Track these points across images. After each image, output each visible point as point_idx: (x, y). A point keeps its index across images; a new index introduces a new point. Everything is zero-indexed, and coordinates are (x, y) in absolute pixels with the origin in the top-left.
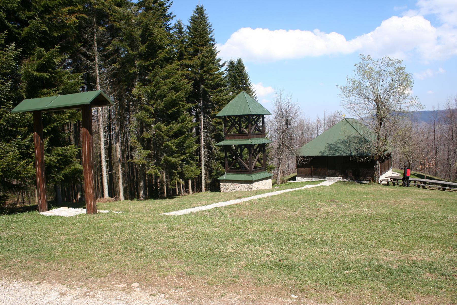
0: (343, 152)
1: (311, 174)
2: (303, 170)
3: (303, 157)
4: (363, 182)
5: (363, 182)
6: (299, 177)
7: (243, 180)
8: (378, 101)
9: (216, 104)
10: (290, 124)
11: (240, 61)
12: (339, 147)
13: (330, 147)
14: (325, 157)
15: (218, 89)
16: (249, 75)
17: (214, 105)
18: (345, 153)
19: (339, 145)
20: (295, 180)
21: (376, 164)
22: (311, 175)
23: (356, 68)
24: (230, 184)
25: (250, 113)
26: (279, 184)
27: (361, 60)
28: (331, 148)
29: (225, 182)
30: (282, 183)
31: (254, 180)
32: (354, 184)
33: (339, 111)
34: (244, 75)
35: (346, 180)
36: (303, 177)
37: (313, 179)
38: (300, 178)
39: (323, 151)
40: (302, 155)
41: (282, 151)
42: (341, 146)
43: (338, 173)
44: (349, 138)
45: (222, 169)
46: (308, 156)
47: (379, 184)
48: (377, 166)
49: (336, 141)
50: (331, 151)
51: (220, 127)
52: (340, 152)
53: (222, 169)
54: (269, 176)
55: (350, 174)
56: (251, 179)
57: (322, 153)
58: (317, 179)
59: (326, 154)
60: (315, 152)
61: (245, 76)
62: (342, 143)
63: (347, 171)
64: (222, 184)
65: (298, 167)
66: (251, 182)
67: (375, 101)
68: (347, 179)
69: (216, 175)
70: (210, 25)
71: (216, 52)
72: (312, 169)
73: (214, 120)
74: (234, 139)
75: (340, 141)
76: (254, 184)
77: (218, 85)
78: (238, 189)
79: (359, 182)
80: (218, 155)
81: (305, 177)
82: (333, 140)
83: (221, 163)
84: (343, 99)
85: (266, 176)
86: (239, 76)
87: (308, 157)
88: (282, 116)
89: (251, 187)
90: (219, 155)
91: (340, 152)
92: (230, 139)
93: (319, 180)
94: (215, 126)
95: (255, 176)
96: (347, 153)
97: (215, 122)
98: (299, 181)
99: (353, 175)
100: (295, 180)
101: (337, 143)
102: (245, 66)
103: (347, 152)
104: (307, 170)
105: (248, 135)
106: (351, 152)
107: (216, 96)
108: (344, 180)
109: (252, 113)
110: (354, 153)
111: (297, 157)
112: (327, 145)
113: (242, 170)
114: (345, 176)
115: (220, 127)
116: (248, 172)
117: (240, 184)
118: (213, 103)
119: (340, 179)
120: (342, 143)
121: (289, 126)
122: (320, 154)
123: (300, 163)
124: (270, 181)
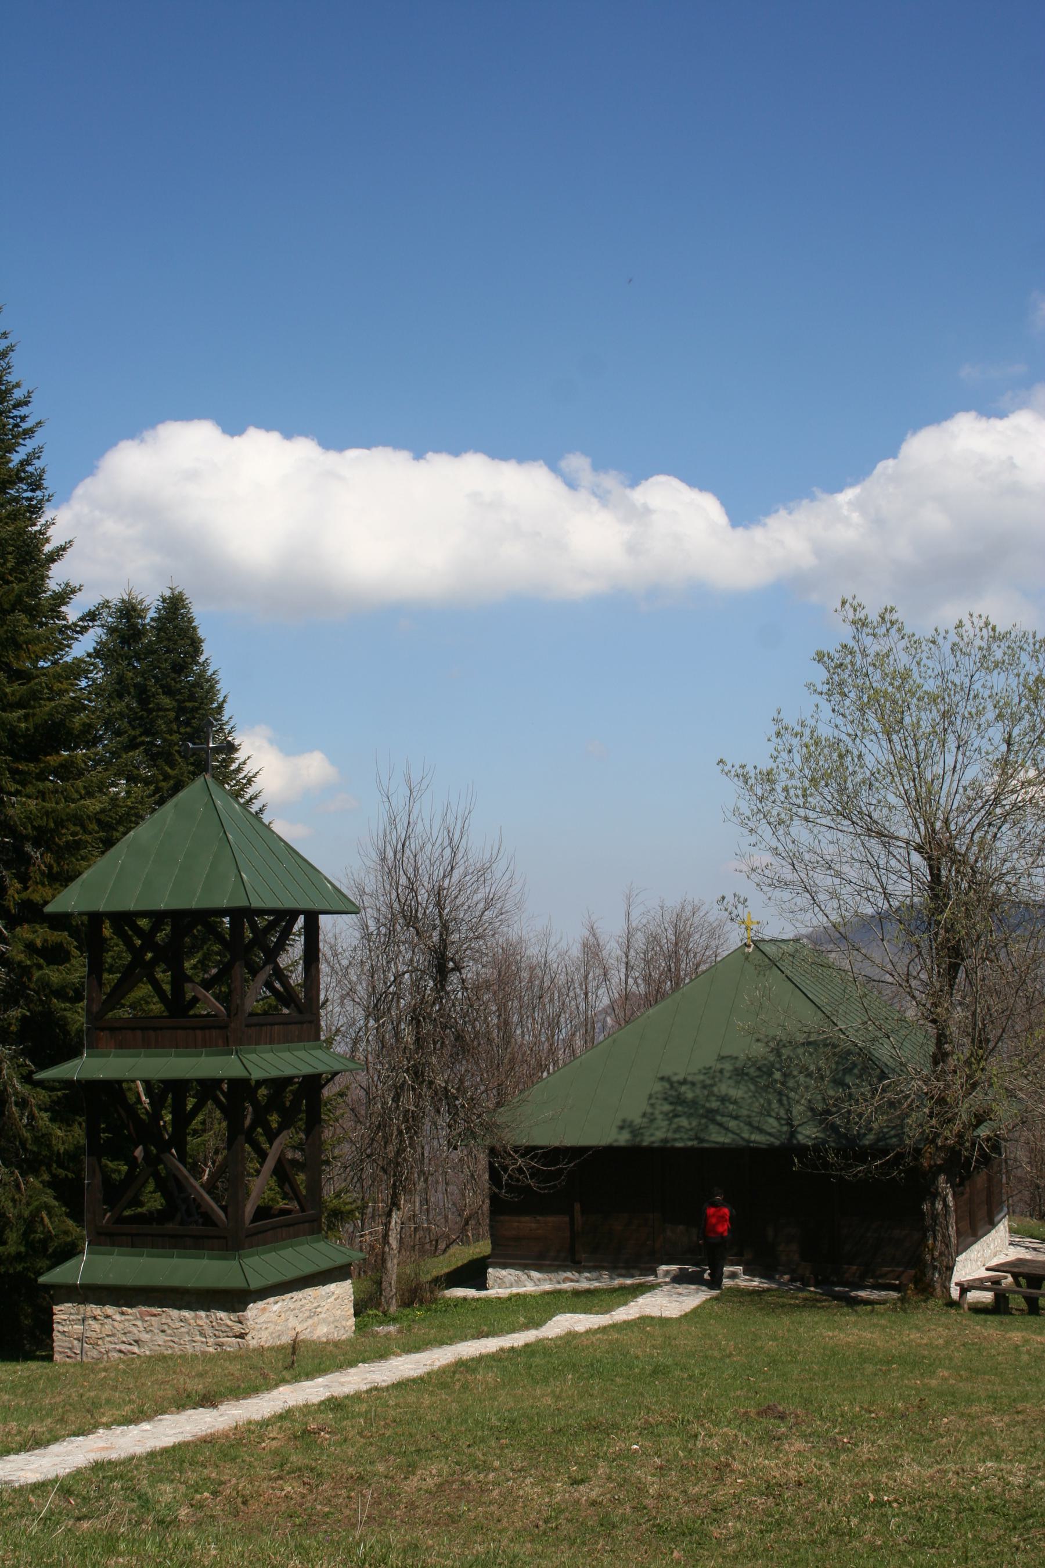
0: (750, 1123)
2: (527, 1224)
3: (529, 1151)
4: (863, 1294)
5: (863, 1294)
6: (504, 1266)
7: (191, 1284)
8: (936, 849)
9: (37, 845)
10: (458, 968)
11: (175, 606)
12: (724, 1099)
13: (675, 1096)
14: (650, 1150)
15: (53, 760)
16: (224, 688)
17: (28, 848)
18: (761, 1131)
19: (724, 1088)
20: (482, 1286)
21: (935, 1195)
22: (569, 1258)
23: (820, 674)
24: (110, 1310)
25: (242, 903)
26: (393, 1309)
27: (849, 630)
28: (679, 1100)
29: (84, 1301)
30: (407, 1303)
31: (255, 1284)
32: (810, 1304)
33: (730, 898)
34: (197, 684)
36: (524, 1267)
37: (585, 1282)
39: (638, 1121)
40: (524, 1141)
41: (413, 1120)
42: (736, 1093)
45: (56, 1223)
46: (557, 1150)
47: (952, 1304)
48: (939, 1206)
50: (684, 1122)
51: (54, 975)
52: (732, 1124)
53: (56, 1223)
54: (341, 1260)
56: (238, 1283)
57: (635, 1132)
58: (603, 1281)
59: (656, 1135)
60: (596, 1128)
61: (199, 693)
62: (740, 1074)
64: (64, 1313)
65: (498, 1207)
66: (236, 1300)
67: (919, 849)
68: (769, 1277)
69: (19, 1257)
70: (18, 394)
71: (47, 548)
73: (24, 932)
74: (147, 1045)
75: (728, 1066)
76: (253, 1310)
77: (55, 735)
78: (161, 1339)
79: (837, 1297)
80: (36, 1140)
81: (539, 1269)
83: (55, 1184)
84: (753, 839)
85: (325, 1265)
86: (168, 692)
87: (554, 1154)
88: (411, 920)
89: (237, 1328)
90: (43, 1139)
91: (732, 1124)
92: (120, 1045)
93: (617, 1282)
94: (26, 971)
95: (261, 1265)
96: (768, 1132)
97: (30, 947)
98: (504, 1292)
100: (482, 1286)
101: (714, 1075)
102: (201, 633)
105: (224, 1027)
107: (42, 795)
108: (756, 1283)
109: (256, 903)
110: (808, 1133)
111: (493, 1151)
112: (658, 1087)
113: (183, 1224)
115: (54, 975)
116: (227, 1241)
117: (175, 1313)
118: (20, 838)
120: (740, 1074)
122: (623, 1139)
123: (510, 1188)
124: (343, 1291)
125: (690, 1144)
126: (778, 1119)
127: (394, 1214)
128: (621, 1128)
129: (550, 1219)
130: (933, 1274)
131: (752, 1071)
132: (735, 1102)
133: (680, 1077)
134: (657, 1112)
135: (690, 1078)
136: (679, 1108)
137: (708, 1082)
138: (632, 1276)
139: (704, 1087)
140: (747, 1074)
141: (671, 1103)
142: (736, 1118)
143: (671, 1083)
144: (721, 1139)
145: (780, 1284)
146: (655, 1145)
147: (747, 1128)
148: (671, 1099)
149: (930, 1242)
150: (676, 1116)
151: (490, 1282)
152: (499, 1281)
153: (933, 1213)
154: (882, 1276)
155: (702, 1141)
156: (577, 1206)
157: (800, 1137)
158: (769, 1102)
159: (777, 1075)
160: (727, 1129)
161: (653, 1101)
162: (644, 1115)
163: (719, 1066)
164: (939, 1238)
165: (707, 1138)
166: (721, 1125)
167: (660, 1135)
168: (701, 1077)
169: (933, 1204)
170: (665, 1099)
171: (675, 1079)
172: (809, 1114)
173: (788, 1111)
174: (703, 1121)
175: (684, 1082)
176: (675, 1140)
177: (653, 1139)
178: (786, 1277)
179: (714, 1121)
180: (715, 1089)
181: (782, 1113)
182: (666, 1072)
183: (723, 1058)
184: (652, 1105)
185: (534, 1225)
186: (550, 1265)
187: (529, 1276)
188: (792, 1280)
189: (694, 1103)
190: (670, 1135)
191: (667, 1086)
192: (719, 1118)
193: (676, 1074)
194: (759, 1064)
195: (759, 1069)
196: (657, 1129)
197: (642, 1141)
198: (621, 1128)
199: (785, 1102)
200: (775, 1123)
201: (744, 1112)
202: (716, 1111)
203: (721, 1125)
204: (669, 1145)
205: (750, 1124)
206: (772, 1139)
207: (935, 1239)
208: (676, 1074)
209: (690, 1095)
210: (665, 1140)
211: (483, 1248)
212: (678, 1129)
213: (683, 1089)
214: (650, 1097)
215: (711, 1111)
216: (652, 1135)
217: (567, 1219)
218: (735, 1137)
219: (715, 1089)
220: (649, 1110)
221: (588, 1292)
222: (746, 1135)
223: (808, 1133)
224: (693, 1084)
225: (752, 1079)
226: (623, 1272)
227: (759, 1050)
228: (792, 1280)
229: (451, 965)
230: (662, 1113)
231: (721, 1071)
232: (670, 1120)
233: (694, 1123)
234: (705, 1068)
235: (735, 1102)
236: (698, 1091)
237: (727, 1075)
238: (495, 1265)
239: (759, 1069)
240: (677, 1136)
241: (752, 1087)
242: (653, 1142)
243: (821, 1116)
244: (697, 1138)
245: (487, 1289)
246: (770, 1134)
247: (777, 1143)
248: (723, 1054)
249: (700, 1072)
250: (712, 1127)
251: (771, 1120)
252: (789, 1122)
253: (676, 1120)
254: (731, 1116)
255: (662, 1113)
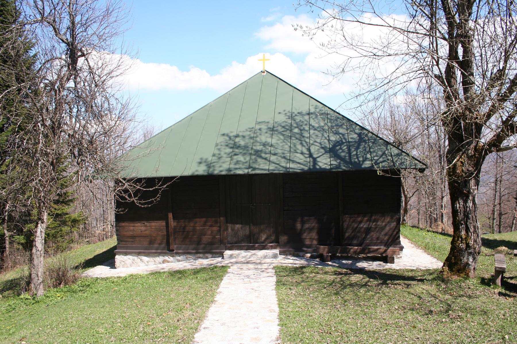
1: (168, 244)
2: (139, 228)
6: (126, 254)
12: (264, 145)
18: (293, 162)
19: (264, 138)
20: (113, 266)
22: (167, 247)
28: (236, 146)
35: (299, 262)
36: (139, 254)
38: (128, 259)
39: (210, 159)
43: (263, 237)
44: (292, 117)
48: (470, 204)
49: (253, 125)
50: (241, 158)
55: (310, 238)
57: (209, 166)
59: (222, 168)
62: (272, 130)
63: (299, 226)
65: (119, 218)
72: (172, 223)
75: (264, 127)
81: (147, 255)
82: (240, 125)
91: (273, 158)
96: (299, 163)
99: (321, 242)
100: (113, 266)
103: (299, 158)
104: (153, 227)
106: (315, 160)
108: (291, 261)
110: (325, 162)
112: (222, 139)
114: (294, 246)
119: (275, 256)
121: (81, 61)
122: (201, 170)
125: (246, 171)
126: (302, 153)
127: (39, 225)
128: (200, 163)
129: (153, 224)
130: (468, 259)
131: (280, 129)
132: (272, 146)
133: (234, 134)
134: (222, 153)
135: (241, 134)
136: (237, 150)
137: (252, 135)
138: (207, 258)
139: (251, 138)
140: (277, 131)
141: (231, 148)
142: (275, 154)
143: (230, 138)
144: (267, 168)
145: (307, 260)
146: (224, 173)
147: (283, 160)
148: (231, 145)
149: (463, 233)
150: (235, 155)
151: (117, 264)
152: (123, 263)
153: (465, 211)
154: (370, 252)
155: (254, 169)
156: (170, 215)
157: (320, 164)
158: (295, 146)
159: (296, 130)
160: (269, 161)
161: (219, 147)
162: (214, 155)
163: (258, 127)
164: (472, 230)
165: (257, 167)
166: (266, 159)
167: (226, 166)
168: (248, 133)
169: (465, 202)
170: (227, 146)
171: (231, 135)
172: (322, 151)
173: (309, 150)
174: (253, 157)
175: (237, 136)
176: (236, 169)
177: (221, 169)
178: (309, 255)
179: (261, 157)
180: (258, 139)
181: (305, 151)
182: (226, 132)
183: (260, 123)
184: (219, 149)
185: (143, 228)
186: (156, 253)
187: (141, 260)
188: (312, 257)
189: (246, 147)
190: (232, 166)
191: (227, 138)
192: (263, 155)
193: (232, 132)
194: (283, 125)
195: (283, 127)
196: (224, 163)
197: (214, 170)
198: (200, 163)
199: (305, 144)
200: (301, 157)
201: (280, 151)
202: (261, 151)
203: (266, 159)
204: (232, 173)
205: (284, 157)
206: (302, 167)
207: (467, 230)
208: (232, 132)
209: (242, 143)
210: (229, 170)
211: (113, 242)
212: (237, 162)
213: (237, 140)
214: (217, 145)
215: (257, 151)
216: (221, 166)
217: (164, 224)
218: (277, 165)
219: (258, 139)
220: (217, 152)
221: (180, 272)
222: (284, 165)
223: (324, 161)
224: (244, 137)
225: (280, 133)
226: (201, 255)
227: (281, 119)
228: (312, 257)
229: (79, 54)
230: (225, 153)
231: (260, 129)
232: (231, 157)
233: (248, 158)
234: (249, 128)
235: (272, 146)
236: (247, 140)
237: (265, 131)
238: (120, 253)
239: (283, 127)
240: (237, 166)
241: (282, 137)
242: (221, 171)
243: (332, 151)
244: (250, 167)
245: (116, 268)
246: (299, 163)
247: (306, 168)
248: (259, 120)
249: (247, 130)
250: (259, 160)
251: (298, 155)
252: (311, 155)
253: (235, 157)
254: (270, 153)
255: (225, 153)
